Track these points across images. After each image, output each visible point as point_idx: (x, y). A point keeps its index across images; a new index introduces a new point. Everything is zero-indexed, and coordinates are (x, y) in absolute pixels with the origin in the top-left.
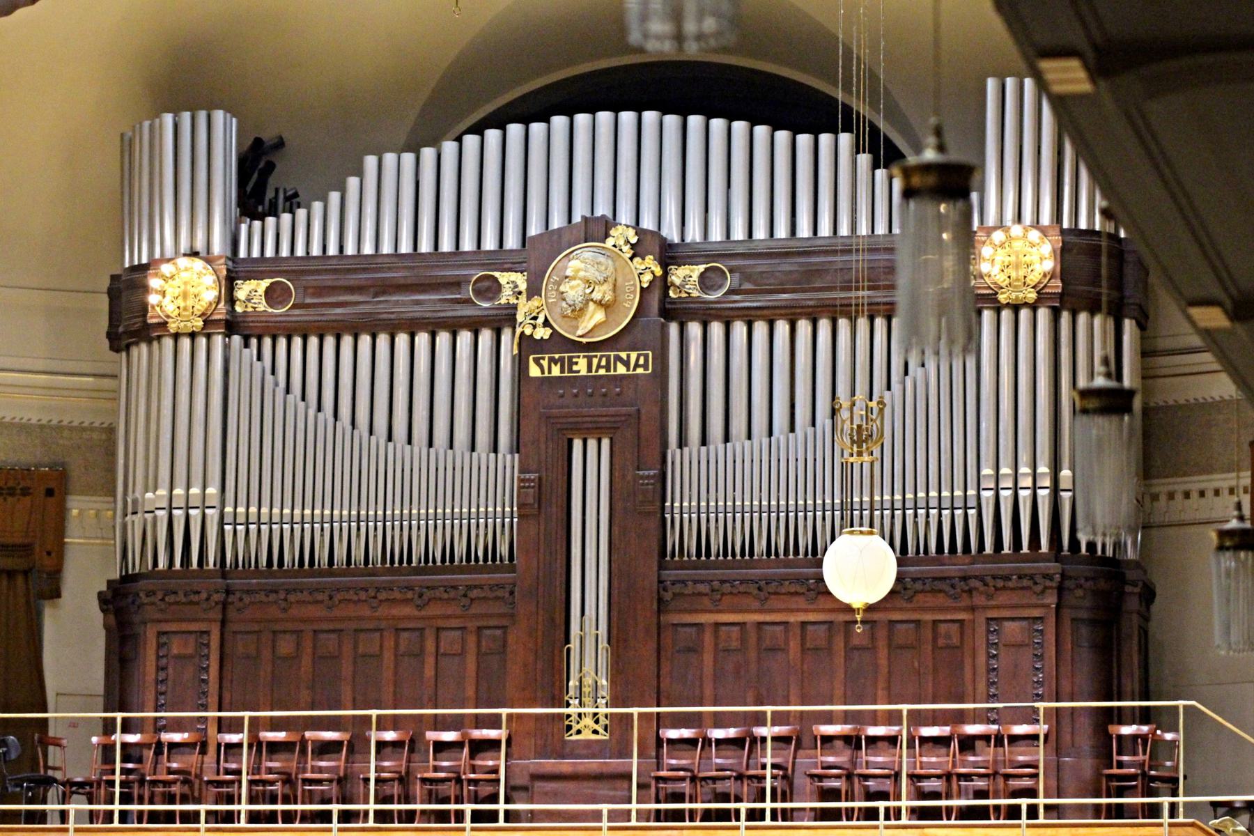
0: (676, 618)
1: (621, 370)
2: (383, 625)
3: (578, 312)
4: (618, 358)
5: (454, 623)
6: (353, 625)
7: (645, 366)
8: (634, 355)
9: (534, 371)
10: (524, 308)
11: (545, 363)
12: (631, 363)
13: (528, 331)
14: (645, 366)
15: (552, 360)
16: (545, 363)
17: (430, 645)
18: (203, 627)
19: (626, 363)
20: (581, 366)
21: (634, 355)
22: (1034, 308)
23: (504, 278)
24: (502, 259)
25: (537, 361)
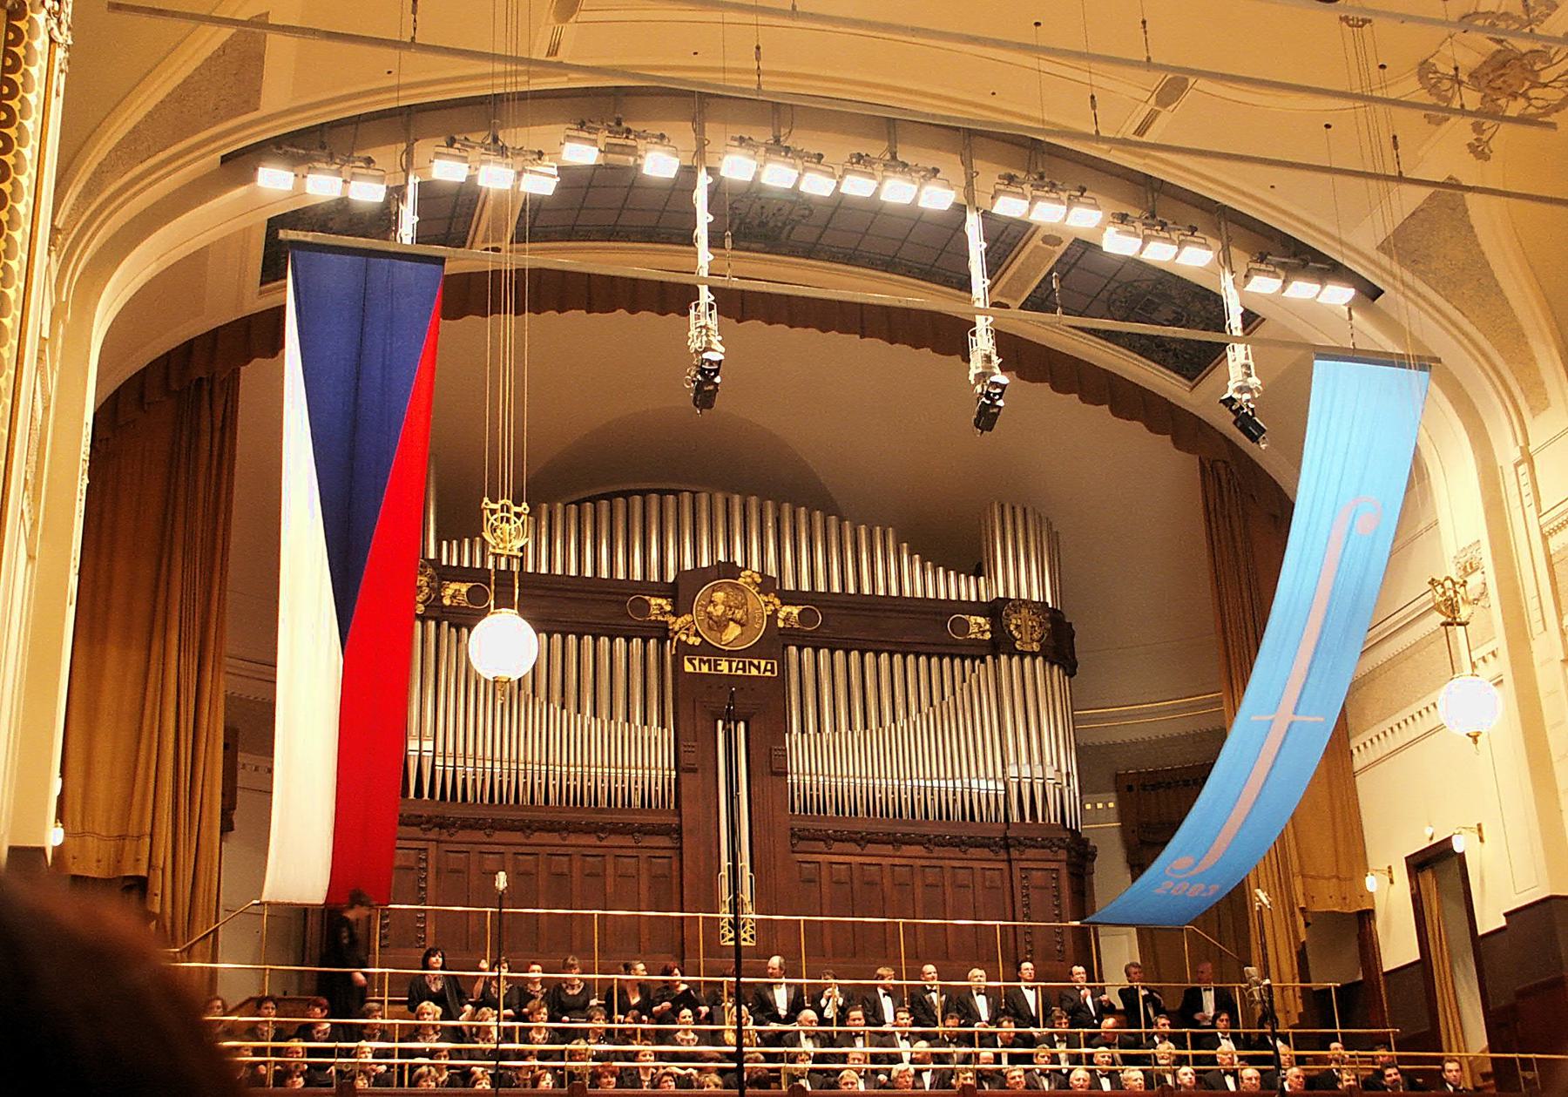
0: (799, 857)
1: (754, 672)
2: (570, 851)
3: (720, 625)
4: (751, 663)
5: (630, 852)
6: (549, 850)
7: (772, 671)
8: (763, 663)
9: (688, 668)
10: (677, 623)
11: (696, 662)
12: (762, 668)
13: (684, 638)
14: (772, 671)
15: (701, 661)
16: (696, 662)
17: (610, 870)
18: (421, 845)
19: (758, 668)
20: (724, 667)
21: (763, 663)
22: (1034, 655)
23: (653, 601)
24: (646, 587)
25: (690, 661)
